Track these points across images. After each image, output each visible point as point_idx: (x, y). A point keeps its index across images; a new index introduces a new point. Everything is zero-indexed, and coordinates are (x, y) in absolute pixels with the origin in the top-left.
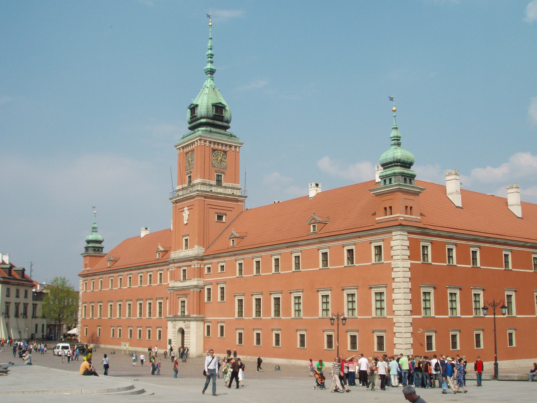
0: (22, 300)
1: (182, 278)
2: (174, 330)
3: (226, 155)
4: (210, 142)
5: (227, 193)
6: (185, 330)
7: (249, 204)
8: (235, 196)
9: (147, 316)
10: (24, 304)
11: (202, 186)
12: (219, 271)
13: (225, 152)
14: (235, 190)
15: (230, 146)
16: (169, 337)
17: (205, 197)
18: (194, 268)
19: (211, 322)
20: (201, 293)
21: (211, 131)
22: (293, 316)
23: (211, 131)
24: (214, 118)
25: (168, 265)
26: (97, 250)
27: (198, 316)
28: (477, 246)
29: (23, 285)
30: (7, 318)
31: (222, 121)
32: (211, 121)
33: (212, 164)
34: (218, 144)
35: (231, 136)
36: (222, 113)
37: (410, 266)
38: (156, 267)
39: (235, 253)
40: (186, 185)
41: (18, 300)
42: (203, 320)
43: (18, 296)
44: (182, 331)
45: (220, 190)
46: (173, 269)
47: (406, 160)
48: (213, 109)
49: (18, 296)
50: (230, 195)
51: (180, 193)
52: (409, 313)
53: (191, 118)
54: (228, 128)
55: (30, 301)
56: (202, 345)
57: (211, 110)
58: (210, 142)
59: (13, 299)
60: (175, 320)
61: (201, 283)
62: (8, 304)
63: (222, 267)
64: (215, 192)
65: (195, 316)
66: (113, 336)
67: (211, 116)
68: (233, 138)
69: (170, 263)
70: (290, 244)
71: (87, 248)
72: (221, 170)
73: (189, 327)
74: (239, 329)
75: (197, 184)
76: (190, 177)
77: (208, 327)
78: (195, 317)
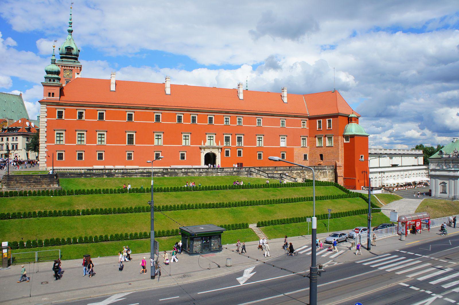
3: (72, 71)
4: (62, 66)
13: (72, 70)
15: (74, 67)
21: (62, 61)
24: (66, 54)
28: (103, 110)
31: (72, 55)
34: (67, 67)
36: (71, 51)
37: (46, 121)
47: (51, 71)
48: (65, 50)
52: (44, 142)
58: (62, 66)
67: (65, 53)
72: (69, 79)
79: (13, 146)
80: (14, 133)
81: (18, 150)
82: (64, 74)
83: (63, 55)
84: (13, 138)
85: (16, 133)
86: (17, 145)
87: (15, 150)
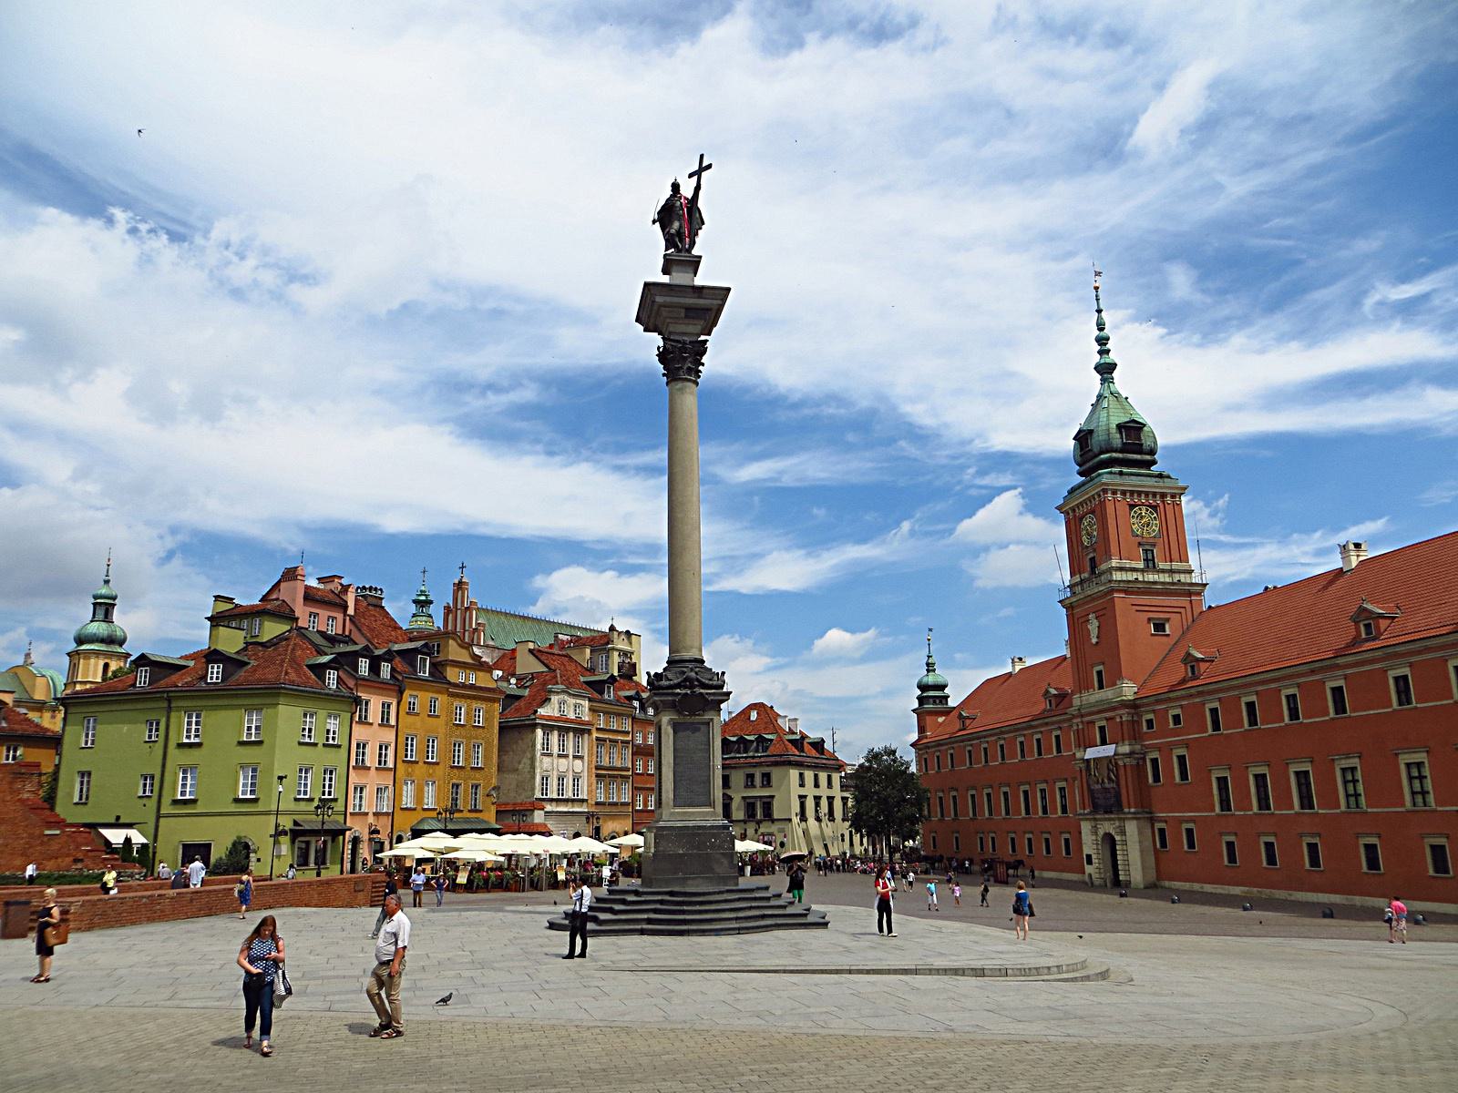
0: (824, 791)
1: (1098, 744)
2: (1094, 838)
4: (1124, 493)
5: (1168, 580)
6: (1117, 838)
7: (1209, 599)
8: (1184, 584)
9: (1040, 813)
10: (828, 798)
11: (1118, 573)
12: (1171, 726)
13: (1155, 508)
14: (1182, 575)
15: (1163, 496)
16: (1086, 851)
17: (1126, 592)
18: (1121, 722)
19: (1166, 822)
20: (1140, 768)
21: (1121, 473)
22: (1343, 808)
23: (1121, 473)
24: (1125, 448)
25: (1070, 720)
26: (938, 701)
27: (1140, 810)
29: (824, 768)
30: (804, 823)
32: (1120, 455)
33: (1133, 531)
34: (1139, 493)
35: (1160, 476)
36: (1140, 439)
38: (1047, 724)
39: (1200, 689)
40: (1086, 575)
41: (817, 792)
42: (1152, 820)
43: (817, 785)
44: (1110, 841)
45: (1151, 577)
46: (1080, 727)
48: (1121, 433)
49: (817, 785)
50: (1173, 584)
51: (1078, 589)
53: (1081, 456)
54: (1154, 462)
55: (837, 792)
56: (1154, 865)
57: (1118, 436)
58: (1124, 493)
59: (810, 791)
60: (1095, 819)
61: (1138, 747)
62: (802, 798)
63: (1177, 719)
64: (1144, 582)
65: (1132, 810)
66: (982, 849)
68: (1166, 480)
69: (1074, 717)
70: (1317, 665)
71: (919, 698)
73: (1123, 833)
74: (1229, 834)
75: (1110, 570)
76: (1093, 560)
77: (1162, 831)
78: (1134, 813)
79: (750, 806)
80: (753, 757)
81: (773, 821)
82: (1132, 521)
83: (1114, 455)
84: (751, 777)
85: (762, 760)
86: (768, 800)
87: (759, 822)
